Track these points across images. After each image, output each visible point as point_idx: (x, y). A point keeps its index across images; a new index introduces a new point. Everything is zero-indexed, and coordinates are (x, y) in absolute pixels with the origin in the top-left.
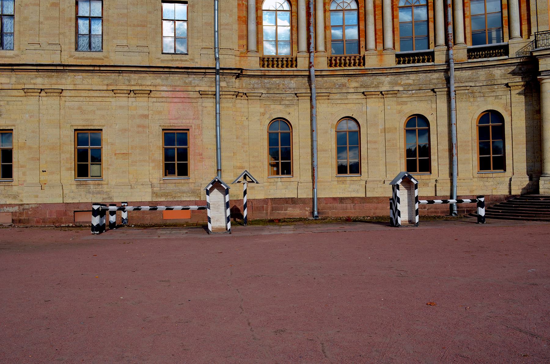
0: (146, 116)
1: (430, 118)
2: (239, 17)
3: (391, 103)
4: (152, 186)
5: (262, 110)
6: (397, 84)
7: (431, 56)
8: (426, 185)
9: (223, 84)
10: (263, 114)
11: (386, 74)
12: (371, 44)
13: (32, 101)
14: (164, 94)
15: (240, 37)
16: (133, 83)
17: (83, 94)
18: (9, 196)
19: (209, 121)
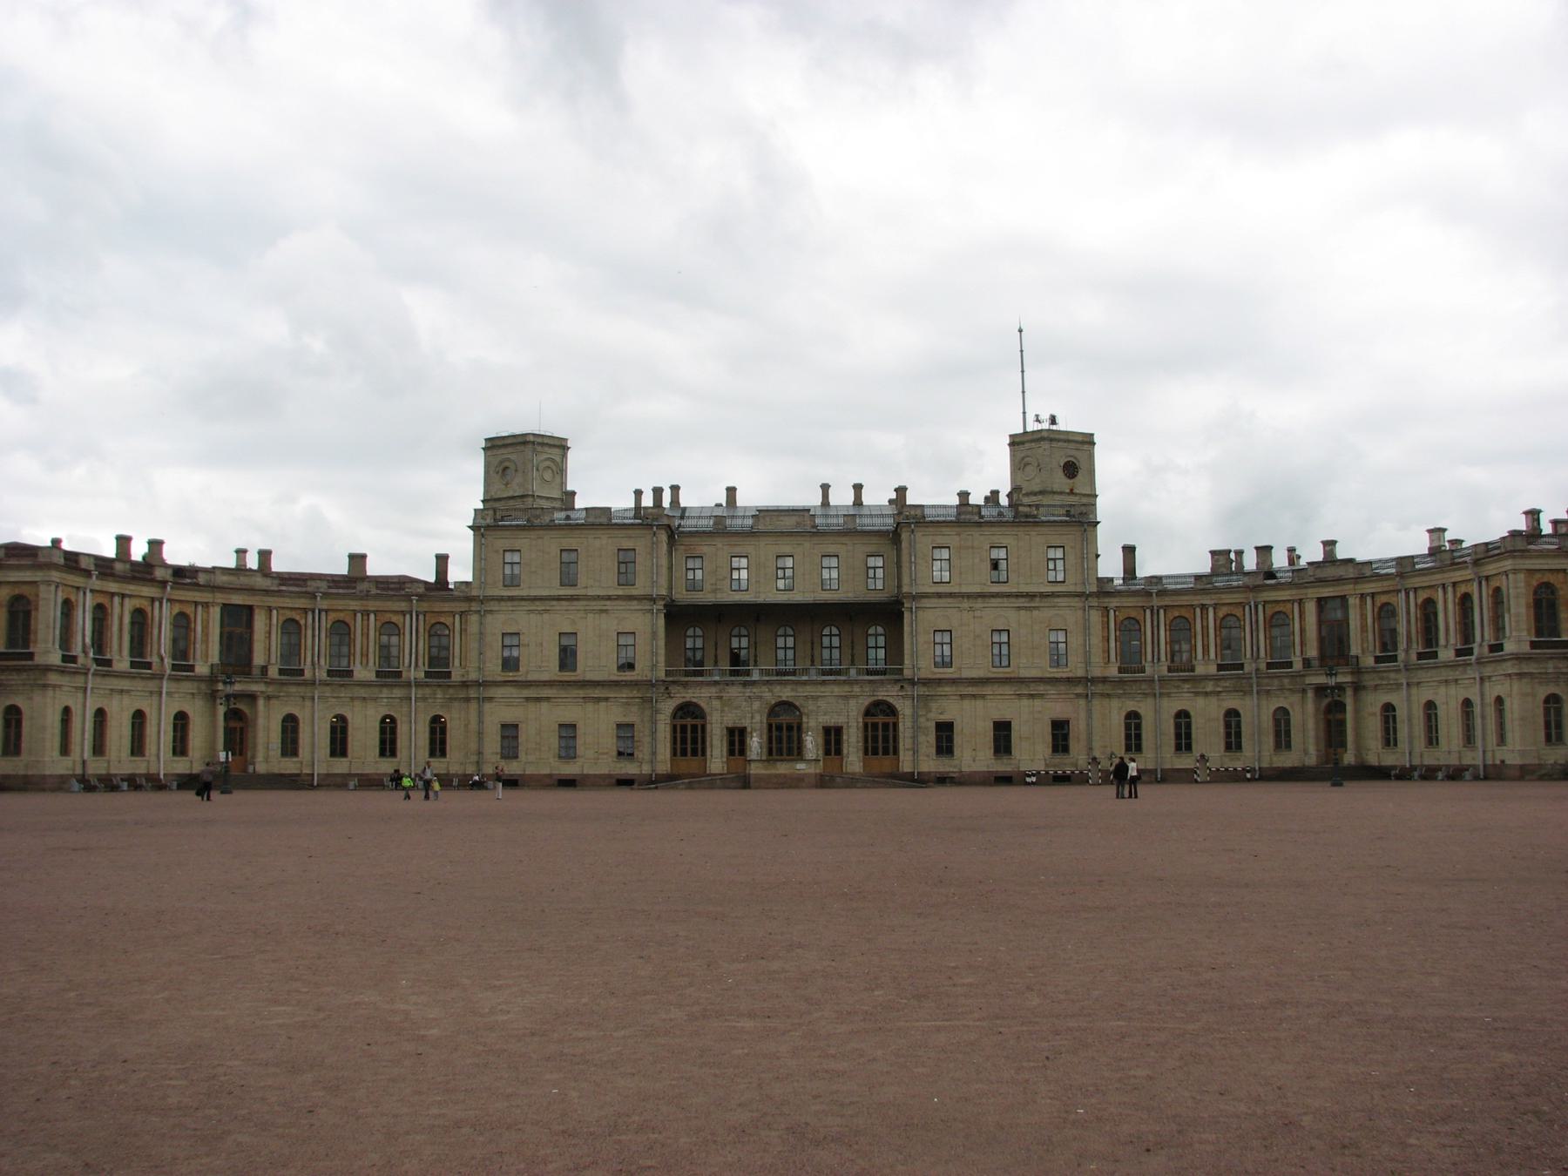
0: (1040, 712)
1: (1241, 712)
2: (1103, 637)
3: (1213, 700)
4: (1045, 760)
5: (1120, 705)
6: (1218, 686)
7: (1241, 666)
8: (1239, 759)
9: (1093, 688)
10: (1121, 708)
11: (1211, 680)
12: (1200, 656)
13: (967, 703)
14: (1052, 696)
15: (1104, 652)
16: (1032, 689)
17: (999, 697)
18: (951, 766)
19: (1083, 715)
